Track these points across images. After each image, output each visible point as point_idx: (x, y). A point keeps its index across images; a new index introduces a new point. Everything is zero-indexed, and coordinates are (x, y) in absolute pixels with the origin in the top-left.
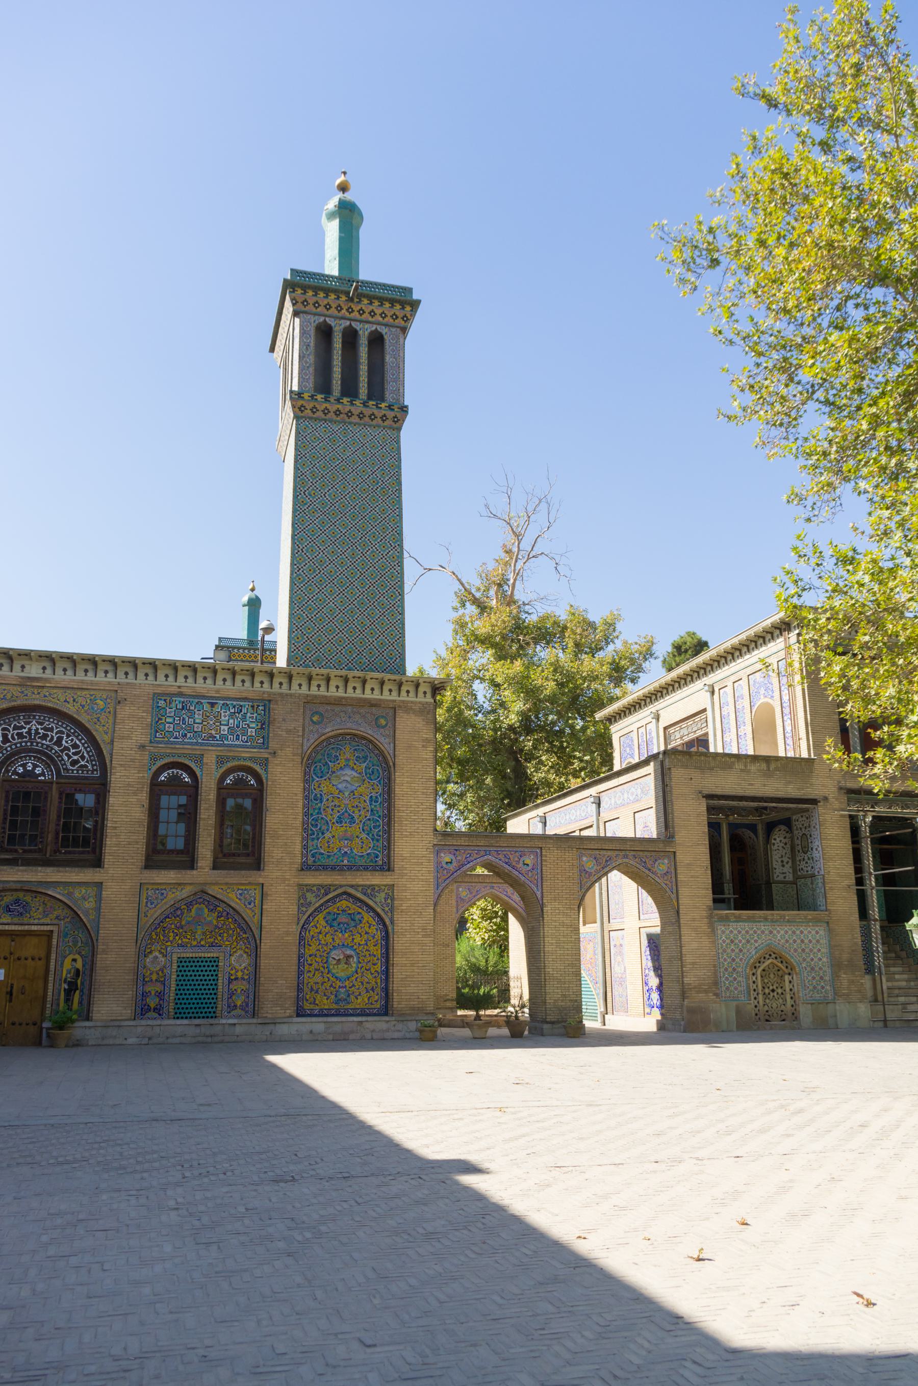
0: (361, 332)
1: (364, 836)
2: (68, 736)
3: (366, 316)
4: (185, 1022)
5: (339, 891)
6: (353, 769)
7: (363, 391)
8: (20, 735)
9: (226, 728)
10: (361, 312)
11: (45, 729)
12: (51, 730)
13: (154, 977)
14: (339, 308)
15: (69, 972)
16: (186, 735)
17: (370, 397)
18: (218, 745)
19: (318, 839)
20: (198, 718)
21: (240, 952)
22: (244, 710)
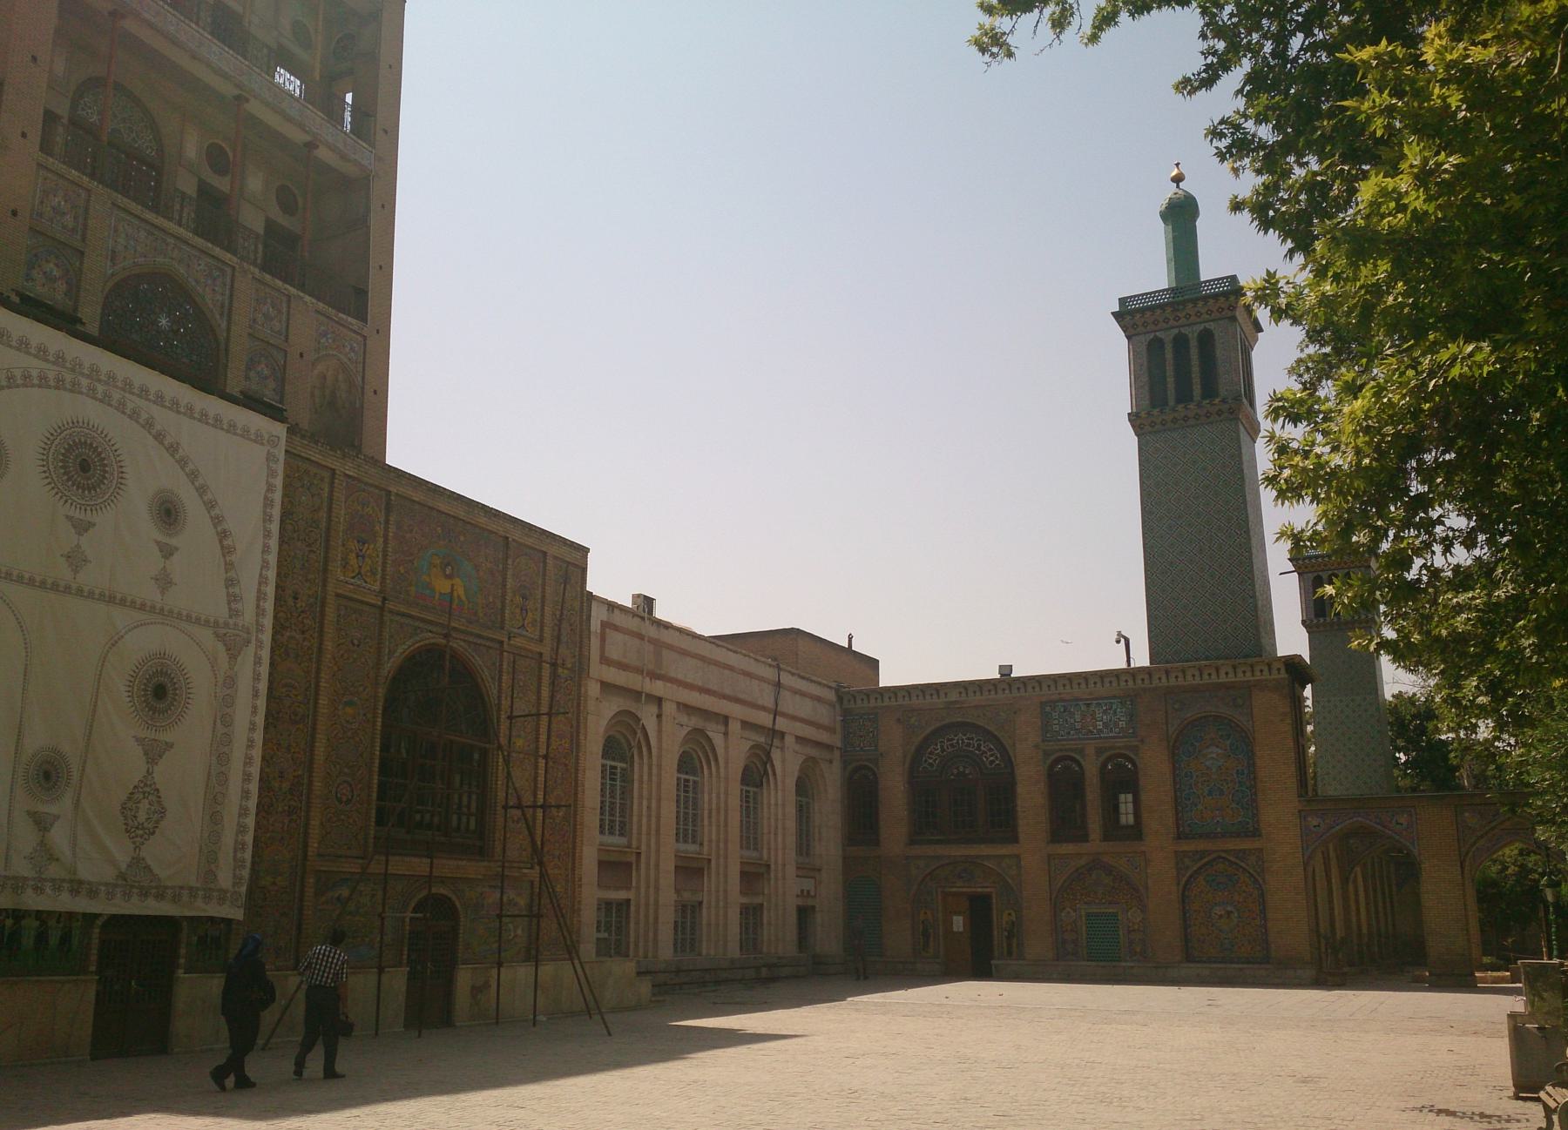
0: (1190, 335)
1: (1234, 805)
2: (985, 743)
3: (1193, 318)
4: (1094, 963)
5: (1214, 855)
6: (1217, 747)
7: (1197, 390)
8: (952, 745)
9: (1101, 723)
10: (1188, 316)
11: (968, 739)
12: (972, 739)
13: (1069, 928)
14: (1166, 320)
15: (1007, 923)
16: (1069, 733)
17: (1204, 397)
18: (1095, 739)
19: (1192, 811)
20: (1078, 717)
21: (1134, 909)
22: (1114, 707)
